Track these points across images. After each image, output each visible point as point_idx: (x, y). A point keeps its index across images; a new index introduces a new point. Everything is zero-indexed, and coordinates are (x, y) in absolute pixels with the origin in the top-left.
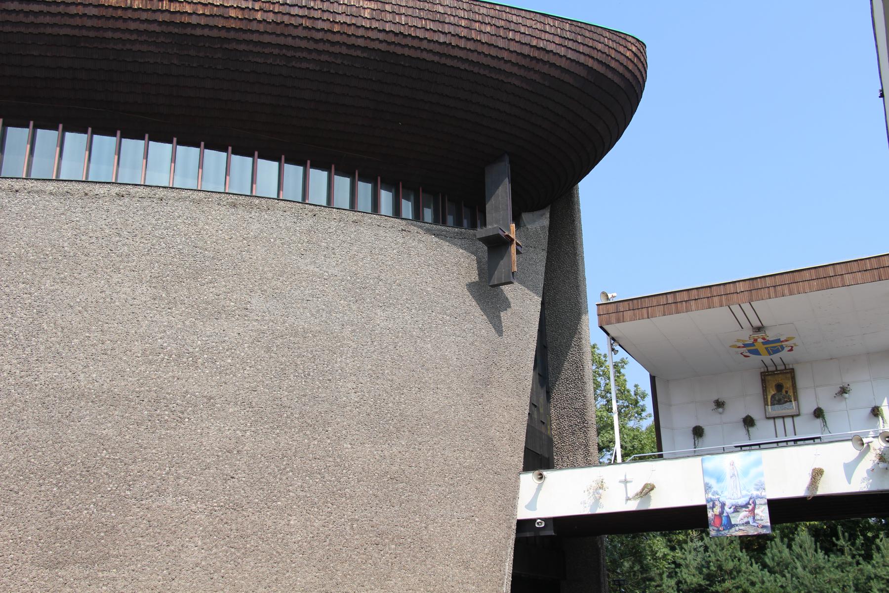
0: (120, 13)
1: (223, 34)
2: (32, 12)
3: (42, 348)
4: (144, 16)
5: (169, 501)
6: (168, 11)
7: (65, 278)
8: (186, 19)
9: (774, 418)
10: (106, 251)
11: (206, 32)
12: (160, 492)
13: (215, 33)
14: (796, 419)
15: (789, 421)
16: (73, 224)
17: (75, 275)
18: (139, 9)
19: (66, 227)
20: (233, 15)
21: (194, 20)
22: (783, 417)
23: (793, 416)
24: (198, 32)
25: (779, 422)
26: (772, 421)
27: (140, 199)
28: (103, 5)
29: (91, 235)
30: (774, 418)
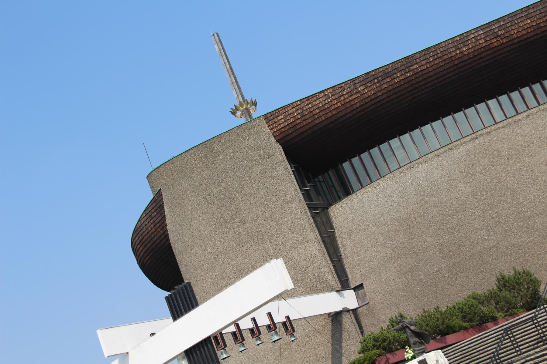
0: (499, 47)
1: (542, 35)
2: (469, 64)
3: (542, 182)
4: (509, 44)
6: (518, 37)
7: (531, 155)
8: (525, 37)
10: (538, 138)
11: (535, 38)
13: (538, 36)
16: (519, 135)
17: (534, 152)
18: (506, 42)
19: (517, 137)
20: (542, 26)
21: (529, 35)
24: (532, 39)
27: (536, 114)
28: (493, 48)
29: (528, 135)
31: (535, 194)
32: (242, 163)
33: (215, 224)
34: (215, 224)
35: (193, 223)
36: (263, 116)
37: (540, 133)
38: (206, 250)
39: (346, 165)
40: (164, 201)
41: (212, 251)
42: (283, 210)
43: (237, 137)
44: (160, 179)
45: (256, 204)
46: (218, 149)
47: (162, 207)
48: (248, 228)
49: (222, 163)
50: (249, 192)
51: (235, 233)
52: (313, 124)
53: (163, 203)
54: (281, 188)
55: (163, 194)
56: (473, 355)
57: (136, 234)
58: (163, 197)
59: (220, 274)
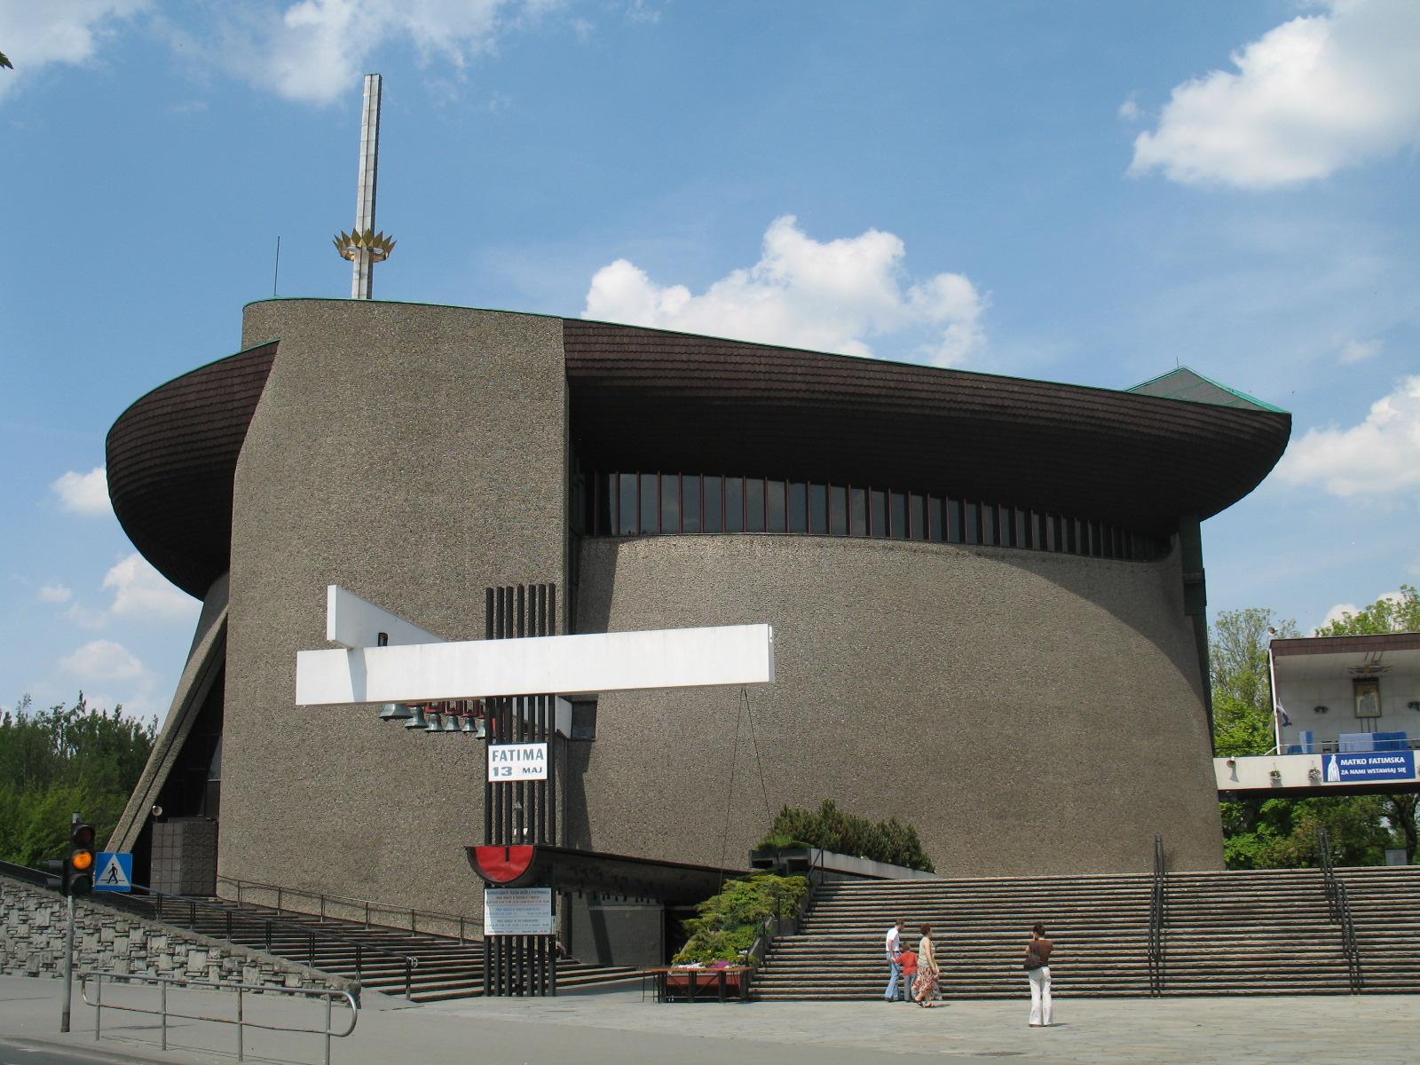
5: (1050, 777)
9: (1361, 718)
12: (1046, 772)
14: (1378, 720)
15: (1373, 719)
22: (1368, 717)
23: (1375, 717)
25: (1365, 721)
26: (1358, 720)
30: (1361, 718)
31: (942, 686)
32: (483, 382)
33: (371, 465)
34: (371, 465)
35: (322, 439)
36: (564, 319)
37: (985, 591)
38: (326, 501)
39: (628, 480)
40: (273, 367)
41: (340, 511)
42: (523, 506)
43: (496, 330)
44: (285, 324)
45: (476, 468)
46: (445, 333)
47: (262, 376)
48: (438, 504)
49: (442, 360)
50: (472, 440)
51: (406, 500)
52: (648, 383)
53: (269, 371)
54: (537, 465)
55: (278, 352)
56: (1023, 904)
57: (161, 396)
58: (276, 360)
59: (335, 560)
